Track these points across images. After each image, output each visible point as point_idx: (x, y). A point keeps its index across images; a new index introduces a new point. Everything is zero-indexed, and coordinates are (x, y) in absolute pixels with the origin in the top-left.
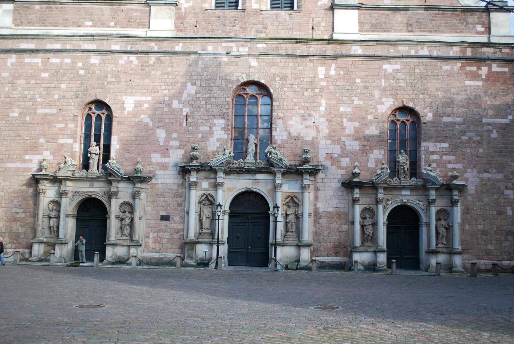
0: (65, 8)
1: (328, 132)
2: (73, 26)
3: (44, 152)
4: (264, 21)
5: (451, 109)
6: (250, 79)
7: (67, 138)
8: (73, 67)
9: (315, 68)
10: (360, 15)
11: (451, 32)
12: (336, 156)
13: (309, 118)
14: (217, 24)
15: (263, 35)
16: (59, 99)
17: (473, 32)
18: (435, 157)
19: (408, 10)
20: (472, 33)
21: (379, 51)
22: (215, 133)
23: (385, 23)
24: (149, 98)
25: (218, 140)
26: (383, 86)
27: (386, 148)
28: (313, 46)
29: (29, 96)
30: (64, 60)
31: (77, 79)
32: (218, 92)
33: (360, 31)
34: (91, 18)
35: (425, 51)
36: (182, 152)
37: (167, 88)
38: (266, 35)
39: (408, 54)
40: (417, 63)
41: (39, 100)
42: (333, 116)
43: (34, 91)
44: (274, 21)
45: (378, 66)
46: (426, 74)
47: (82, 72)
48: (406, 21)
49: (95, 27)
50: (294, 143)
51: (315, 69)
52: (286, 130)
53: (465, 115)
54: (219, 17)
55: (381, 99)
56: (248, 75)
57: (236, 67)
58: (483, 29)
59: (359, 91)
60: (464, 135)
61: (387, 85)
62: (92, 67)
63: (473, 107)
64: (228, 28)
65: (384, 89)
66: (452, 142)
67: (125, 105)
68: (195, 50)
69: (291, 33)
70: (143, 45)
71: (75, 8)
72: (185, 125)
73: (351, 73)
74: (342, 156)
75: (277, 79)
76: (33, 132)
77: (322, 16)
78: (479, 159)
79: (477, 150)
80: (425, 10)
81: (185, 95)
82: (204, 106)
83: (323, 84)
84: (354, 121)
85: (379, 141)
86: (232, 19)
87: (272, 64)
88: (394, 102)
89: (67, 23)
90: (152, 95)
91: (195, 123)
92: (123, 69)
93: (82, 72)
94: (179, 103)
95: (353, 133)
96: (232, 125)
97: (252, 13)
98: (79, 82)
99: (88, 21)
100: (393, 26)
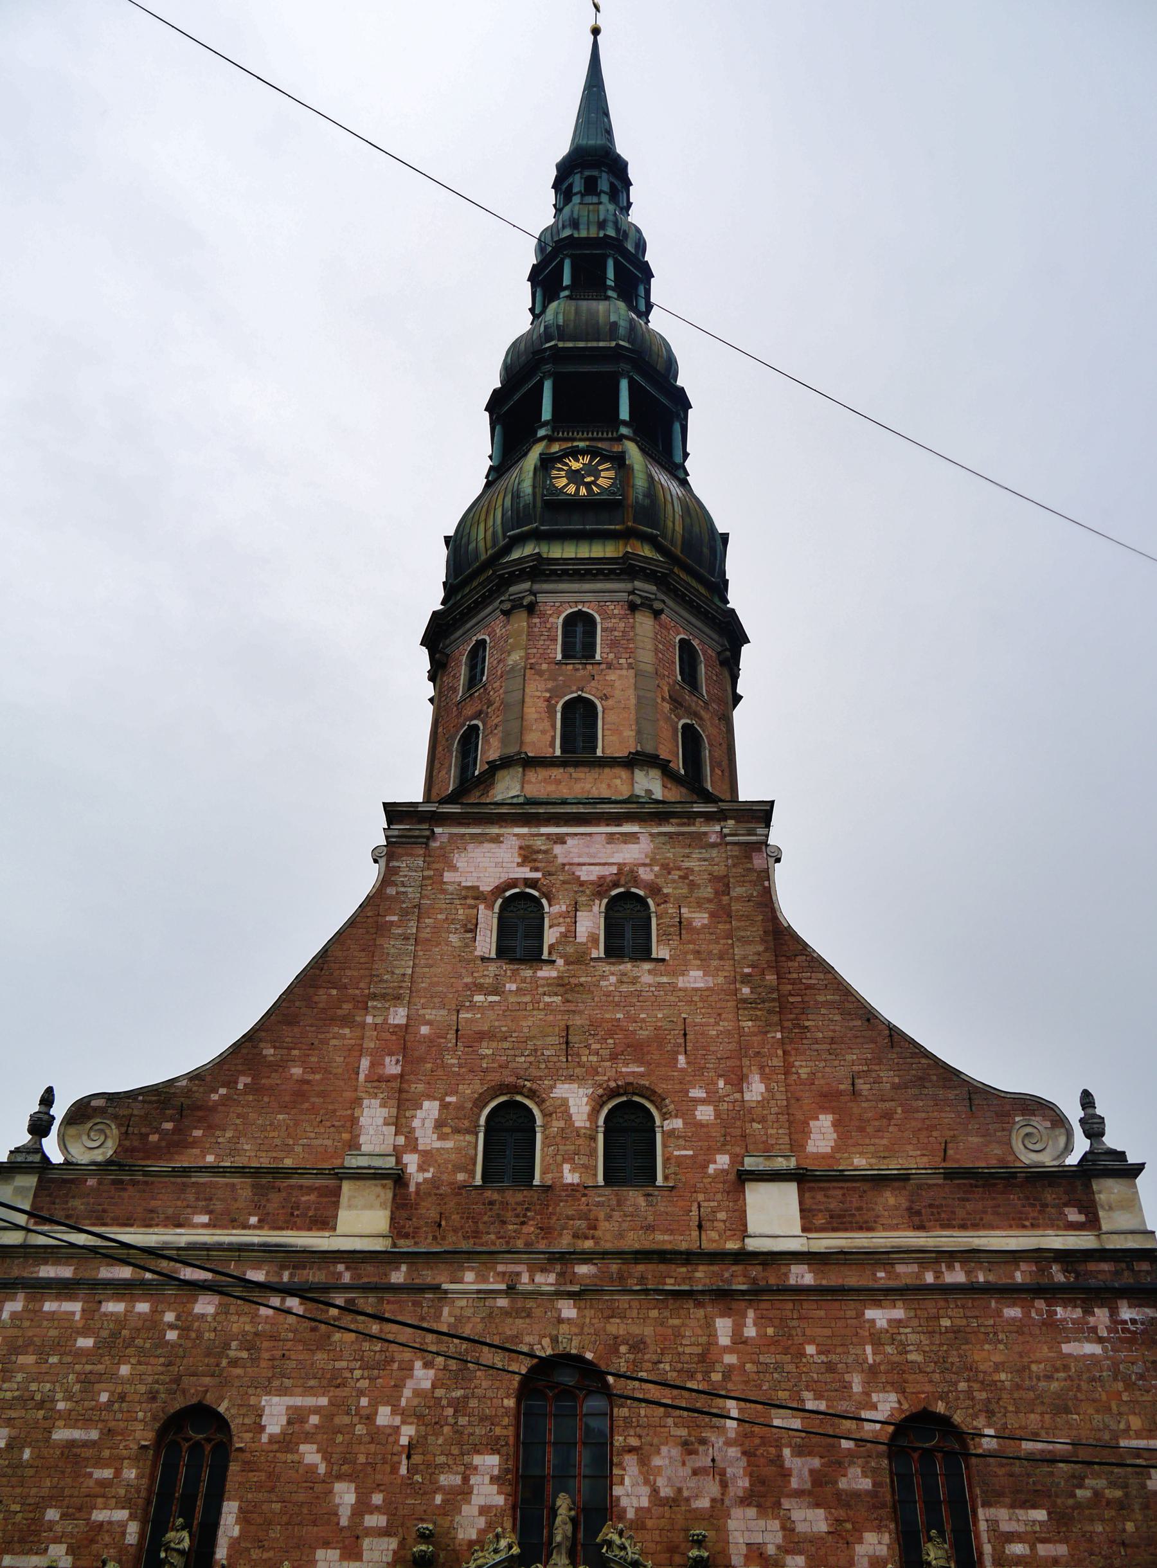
0: (152, 1183)
1: (747, 1485)
2: (166, 1226)
3: (52, 1546)
4: (590, 1211)
5: (1038, 1417)
6: (560, 1350)
7: (116, 1508)
8: (152, 1324)
9: (709, 1320)
11: (1011, 1226)
12: (771, 1550)
13: (701, 1448)
14: (486, 1218)
15: (588, 1244)
16: (110, 1402)
17: (1061, 1223)
18: (1018, 1549)
19: (909, 1179)
20: (1059, 1228)
21: (852, 1278)
22: (475, 1492)
23: (859, 1209)
24: (323, 1401)
25: (484, 1510)
26: (870, 1361)
27: (892, 1526)
28: (701, 1268)
29: (38, 1397)
30: (134, 1307)
31: (159, 1351)
32: (485, 1384)
33: (804, 1230)
35: (956, 1276)
36: (393, 1543)
37: (366, 1374)
38: (596, 1243)
39: (918, 1282)
40: (942, 1304)
41: (61, 1406)
42: (757, 1441)
43: (53, 1383)
44: (613, 1210)
45: (852, 1313)
46: (968, 1329)
47: (172, 1335)
48: (905, 1204)
49: (215, 1226)
50: (667, 1515)
51: (709, 1325)
52: (647, 1482)
53: (1074, 1433)
54: (491, 1203)
55: (868, 1394)
56: (555, 1340)
57: (528, 1321)
58: (1081, 1218)
59: (815, 1376)
60: (1081, 1486)
61: (878, 1358)
62: (196, 1324)
63: (1091, 1411)
64: (511, 1227)
65: (872, 1371)
66: (1054, 1505)
67: (264, 1418)
68: (436, 1282)
69: (651, 1238)
70: (320, 1269)
71: (173, 1183)
72: (403, 1471)
73: (794, 1333)
74: (788, 1552)
75: (623, 1349)
76: (34, 1491)
77: (719, 1196)
78: (1129, 1551)
79: (1120, 1527)
81: (407, 1392)
82: (451, 1420)
83: (730, 1359)
84: (810, 1454)
85: (875, 1507)
86: (519, 1209)
87: (610, 1312)
88: (899, 1402)
89: (152, 1219)
90: (331, 1394)
91: (428, 1466)
92: (268, 1327)
93: (172, 1335)
94: (393, 1413)
95: (808, 1486)
96: (517, 1469)
97: (564, 1194)
98: (162, 1360)
99: (201, 1213)
100: (878, 1217)
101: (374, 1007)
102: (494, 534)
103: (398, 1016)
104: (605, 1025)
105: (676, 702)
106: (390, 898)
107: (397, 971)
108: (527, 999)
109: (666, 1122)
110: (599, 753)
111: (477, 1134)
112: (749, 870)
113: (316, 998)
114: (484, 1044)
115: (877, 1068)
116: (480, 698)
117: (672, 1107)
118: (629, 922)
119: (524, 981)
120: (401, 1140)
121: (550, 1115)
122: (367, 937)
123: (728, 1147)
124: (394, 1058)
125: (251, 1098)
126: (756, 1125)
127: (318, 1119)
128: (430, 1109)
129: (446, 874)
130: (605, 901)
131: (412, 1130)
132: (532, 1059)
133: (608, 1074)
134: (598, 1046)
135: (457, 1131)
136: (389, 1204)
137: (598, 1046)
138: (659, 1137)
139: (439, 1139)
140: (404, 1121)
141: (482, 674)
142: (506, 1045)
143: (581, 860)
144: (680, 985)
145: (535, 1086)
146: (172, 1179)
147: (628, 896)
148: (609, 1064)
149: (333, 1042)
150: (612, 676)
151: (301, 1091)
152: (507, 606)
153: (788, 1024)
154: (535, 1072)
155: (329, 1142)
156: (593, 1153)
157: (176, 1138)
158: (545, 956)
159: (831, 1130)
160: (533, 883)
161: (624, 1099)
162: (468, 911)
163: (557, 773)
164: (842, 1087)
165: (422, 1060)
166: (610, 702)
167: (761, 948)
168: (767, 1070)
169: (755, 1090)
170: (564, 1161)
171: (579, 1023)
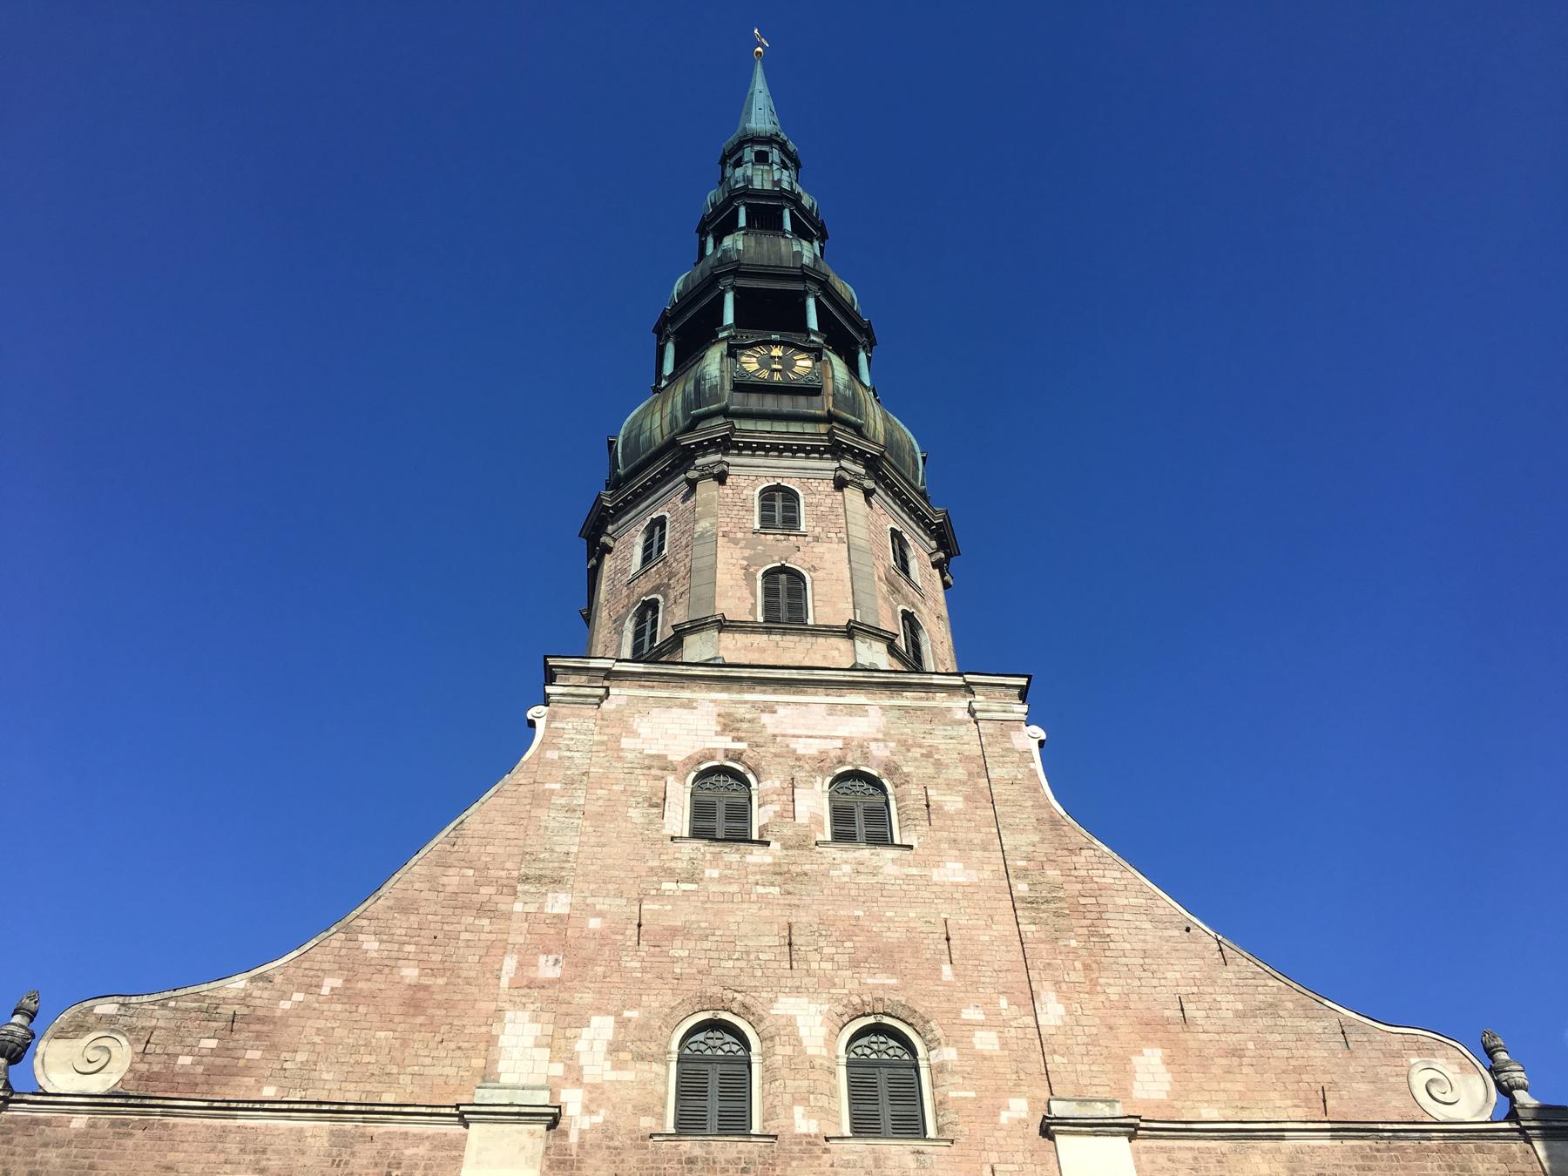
10: (1136, 1153)
19: (1282, 1138)
34: (258, 1162)
54: (691, 1161)
71: (208, 1127)
77: (1019, 1157)
80: (1333, 1138)
97: (796, 1148)
101: (525, 893)
102: (674, 419)
103: (559, 903)
104: (839, 924)
105: (894, 589)
106: (552, 763)
107: (557, 849)
108: (735, 888)
109: (933, 1053)
110: (810, 621)
111: (667, 1065)
112: (1008, 750)
113: (445, 880)
114: (677, 943)
115: (1211, 990)
116: (658, 572)
117: (939, 1033)
118: (862, 807)
119: (729, 866)
120: (558, 1069)
121: (772, 1039)
122: (518, 808)
123: (1024, 1089)
124: (552, 958)
125: (339, 1007)
126: (1056, 1057)
127: (438, 1038)
128: (602, 1028)
129: (623, 740)
130: (829, 779)
131: (573, 1056)
132: (743, 964)
133: (849, 986)
134: (833, 950)
135: (641, 1057)
136: (539, 1160)
137: (833, 950)
138: (924, 1073)
139: (614, 1068)
140: (563, 1042)
141: (661, 548)
142: (707, 945)
143: (797, 732)
144: (935, 878)
145: (748, 1001)
146: (207, 1121)
147: (857, 775)
148: (849, 973)
149: (465, 936)
150: (820, 548)
151: (416, 1000)
152: (692, 474)
153: (1085, 931)
154: (747, 981)
155: (452, 1071)
156: (832, 1094)
157: (219, 1061)
158: (755, 837)
159: (1163, 1069)
160: (737, 757)
161: (871, 1020)
162: (651, 783)
163: (761, 640)
164: (1167, 1013)
165: (589, 962)
166: (819, 574)
167: (1036, 838)
168: (1064, 986)
169: (1052, 1012)
170: (795, 1101)
171: (804, 920)
